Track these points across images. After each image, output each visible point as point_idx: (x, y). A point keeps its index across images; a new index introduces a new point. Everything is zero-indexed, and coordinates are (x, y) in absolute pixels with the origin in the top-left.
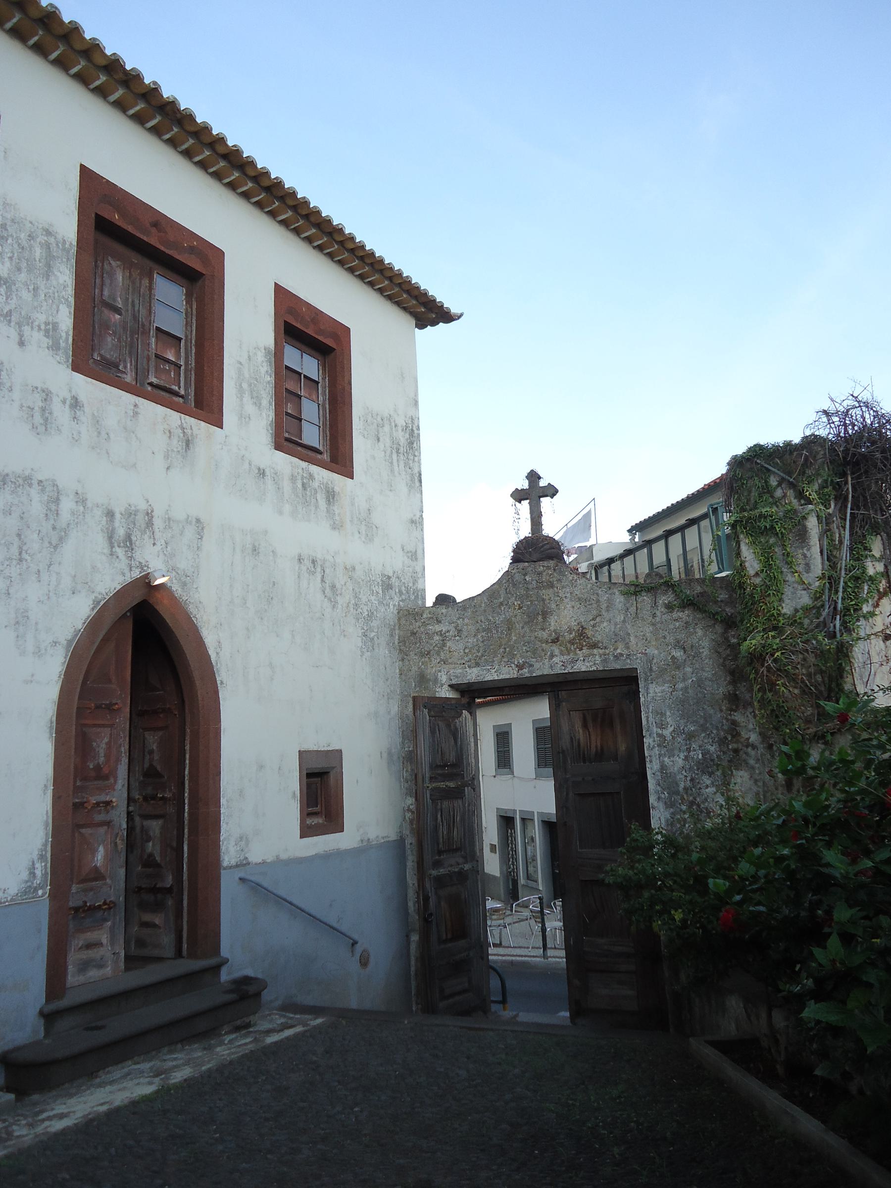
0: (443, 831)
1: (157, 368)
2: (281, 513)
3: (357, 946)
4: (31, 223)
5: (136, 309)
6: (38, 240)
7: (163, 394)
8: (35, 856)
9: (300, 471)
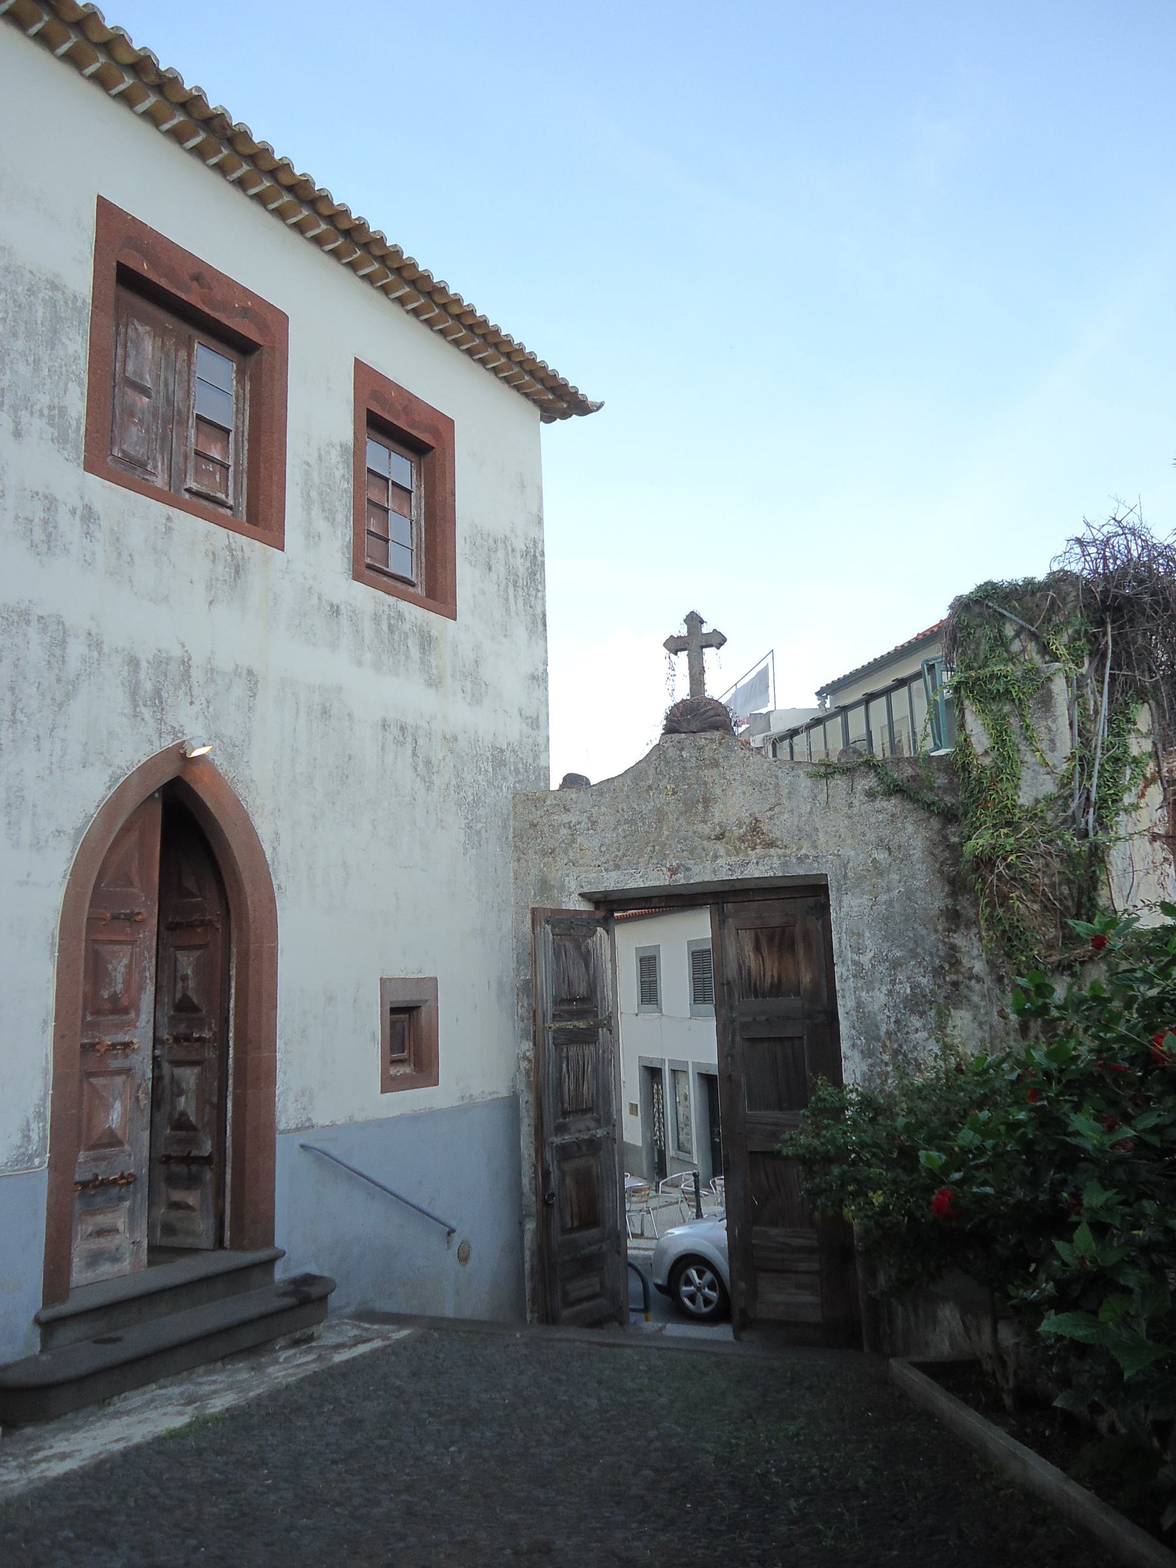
0: (569, 1086)
1: (197, 470)
2: (359, 664)
3: (455, 1236)
4: (31, 272)
5: (171, 388)
7: (204, 504)
8: (30, 1114)
9: (386, 608)
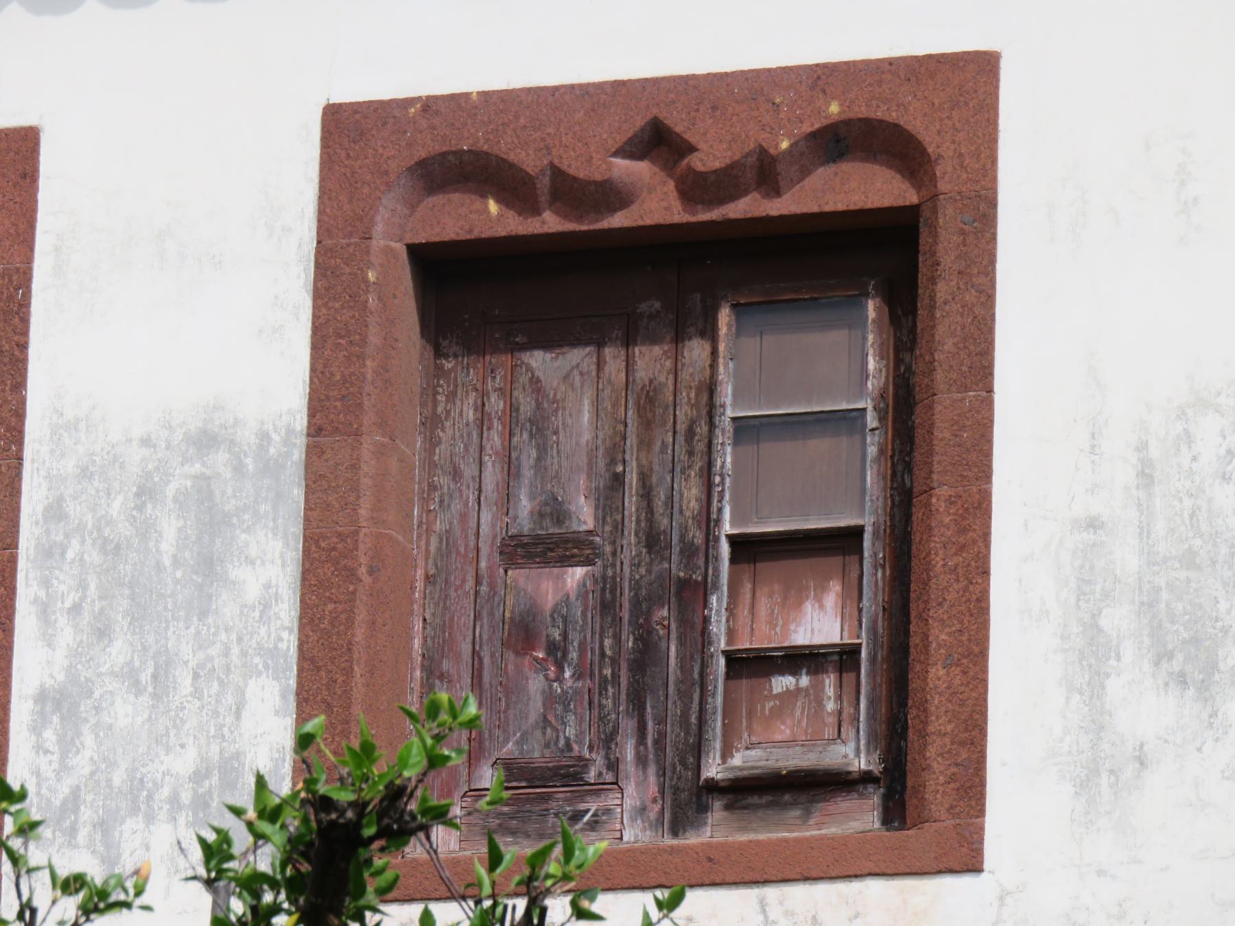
4: (146, 442)
6: (170, 491)
